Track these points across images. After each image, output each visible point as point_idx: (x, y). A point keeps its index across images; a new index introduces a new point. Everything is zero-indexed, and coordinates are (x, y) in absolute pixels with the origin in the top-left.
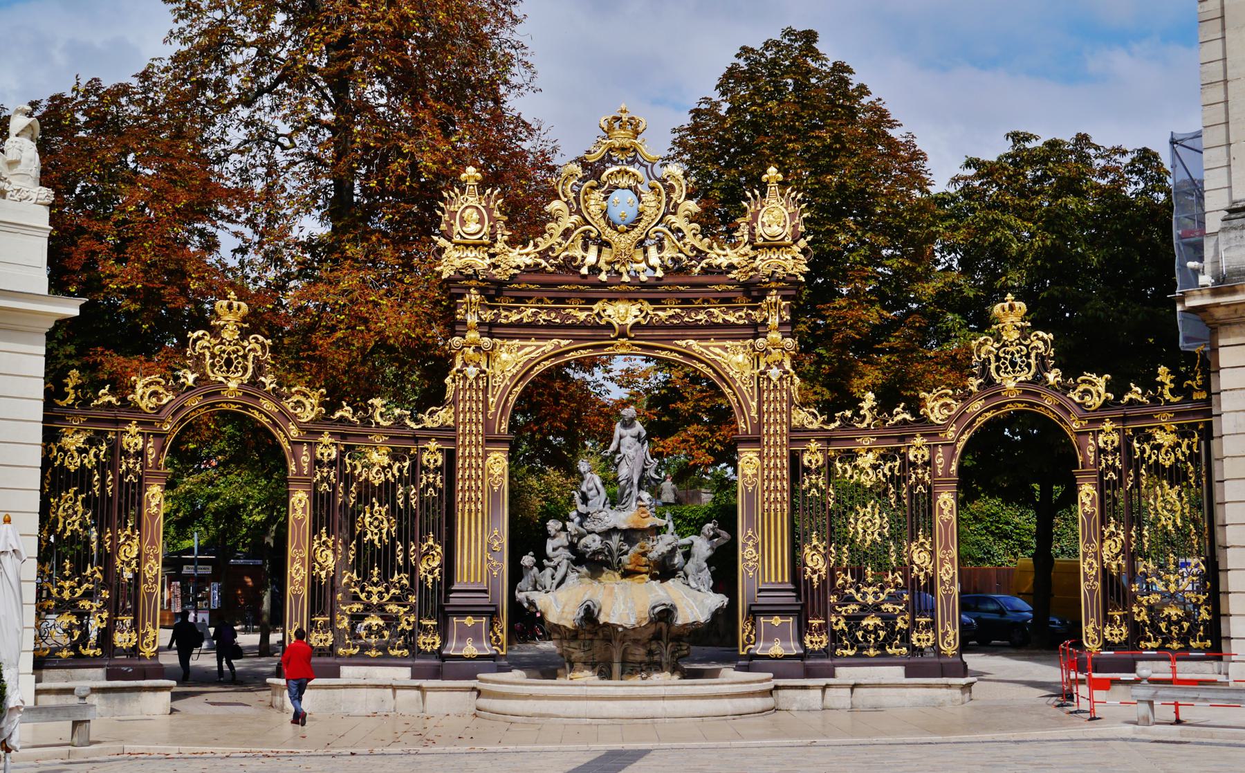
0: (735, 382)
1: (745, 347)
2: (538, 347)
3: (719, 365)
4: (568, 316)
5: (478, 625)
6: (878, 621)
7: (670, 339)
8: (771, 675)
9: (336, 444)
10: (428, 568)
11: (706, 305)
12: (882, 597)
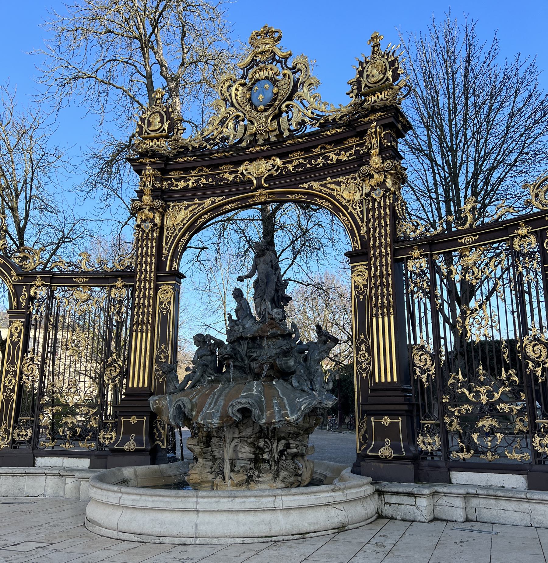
0: (347, 209)
1: (355, 179)
2: (200, 205)
3: (334, 197)
4: (222, 179)
5: (140, 423)
6: (495, 423)
7: (295, 185)
8: (370, 479)
9: (47, 285)
10: (111, 377)
11: (323, 151)
12: (497, 396)
